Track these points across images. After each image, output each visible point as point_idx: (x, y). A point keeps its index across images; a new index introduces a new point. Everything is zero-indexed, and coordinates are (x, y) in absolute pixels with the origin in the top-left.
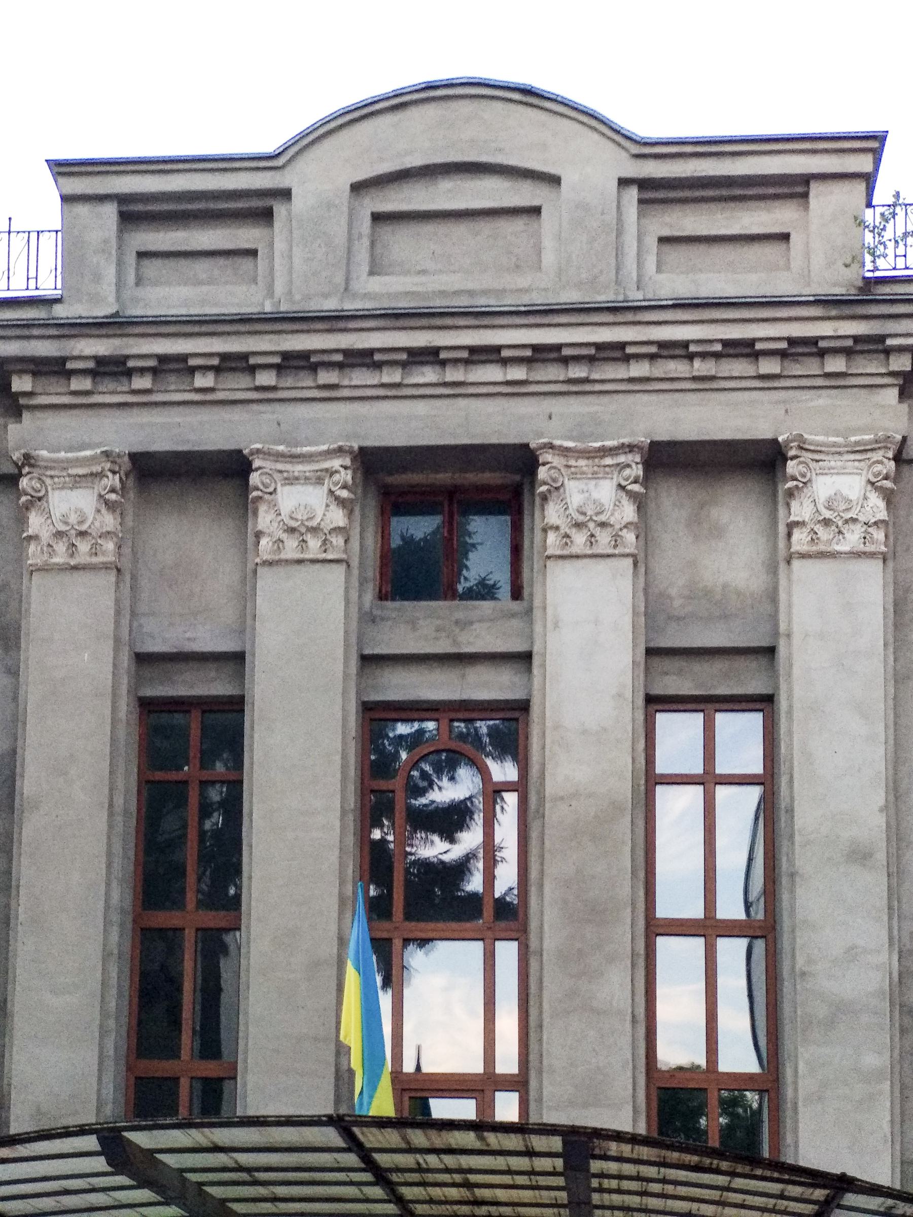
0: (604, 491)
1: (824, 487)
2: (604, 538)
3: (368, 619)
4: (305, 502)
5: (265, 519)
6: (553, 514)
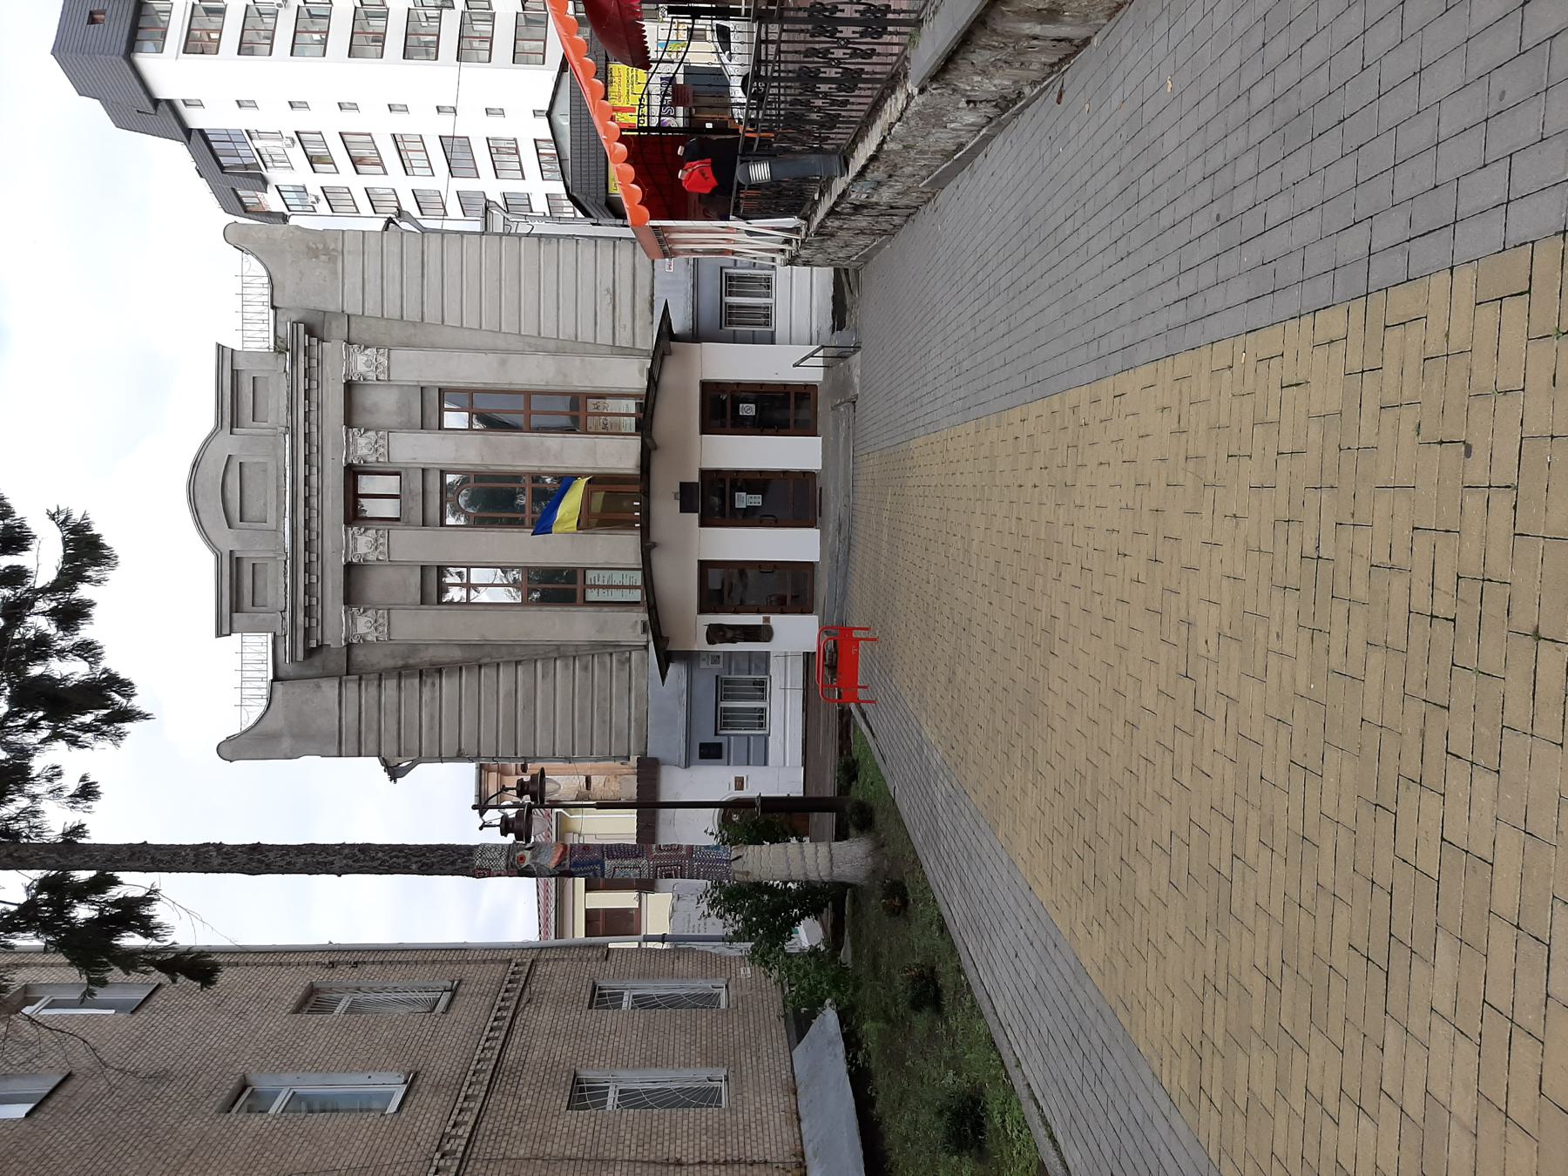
0: (362, 441)
1: (361, 368)
2: (381, 442)
3: (408, 523)
4: (364, 544)
5: (370, 557)
6: (372, 459)
